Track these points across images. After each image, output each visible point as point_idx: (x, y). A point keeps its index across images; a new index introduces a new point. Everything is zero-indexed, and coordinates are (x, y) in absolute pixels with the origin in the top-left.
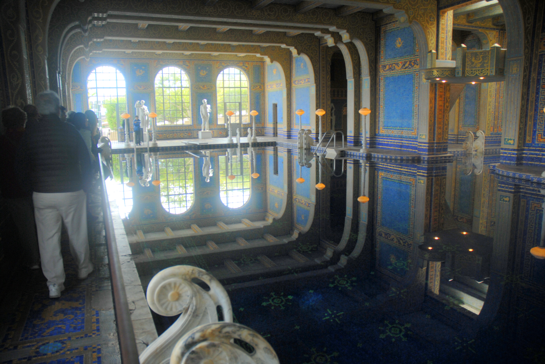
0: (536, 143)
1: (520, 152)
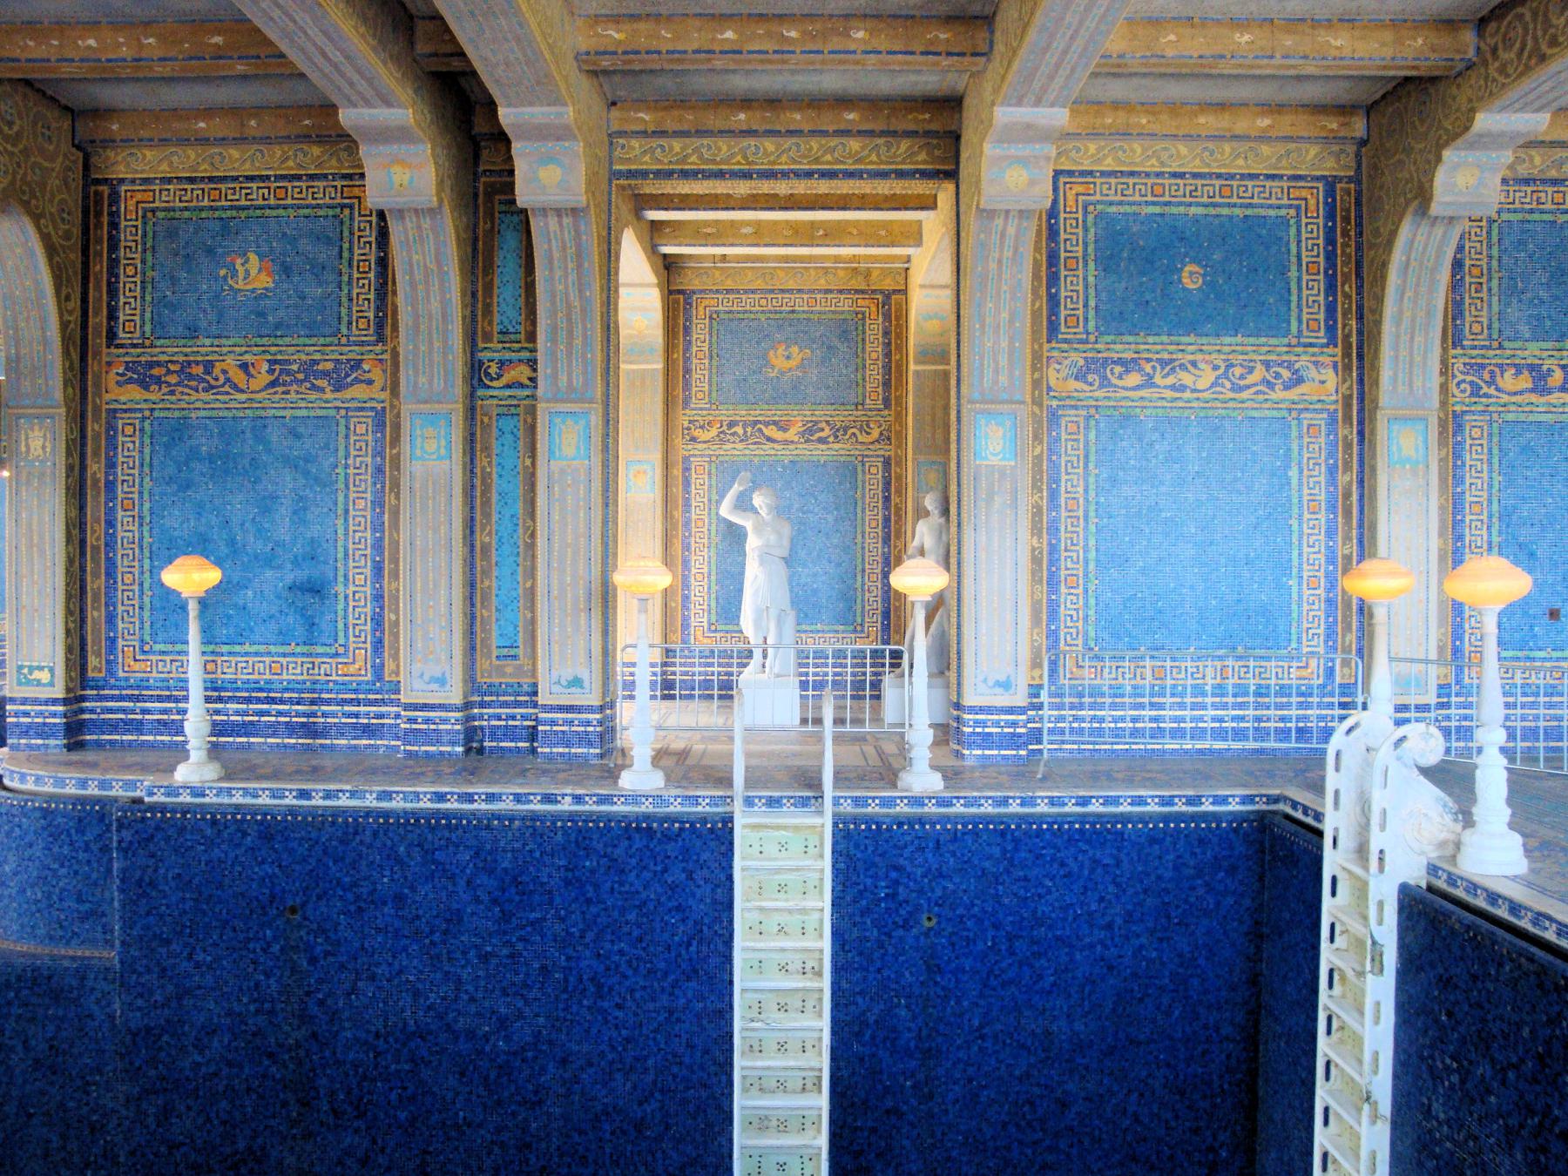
1: (75, 707)
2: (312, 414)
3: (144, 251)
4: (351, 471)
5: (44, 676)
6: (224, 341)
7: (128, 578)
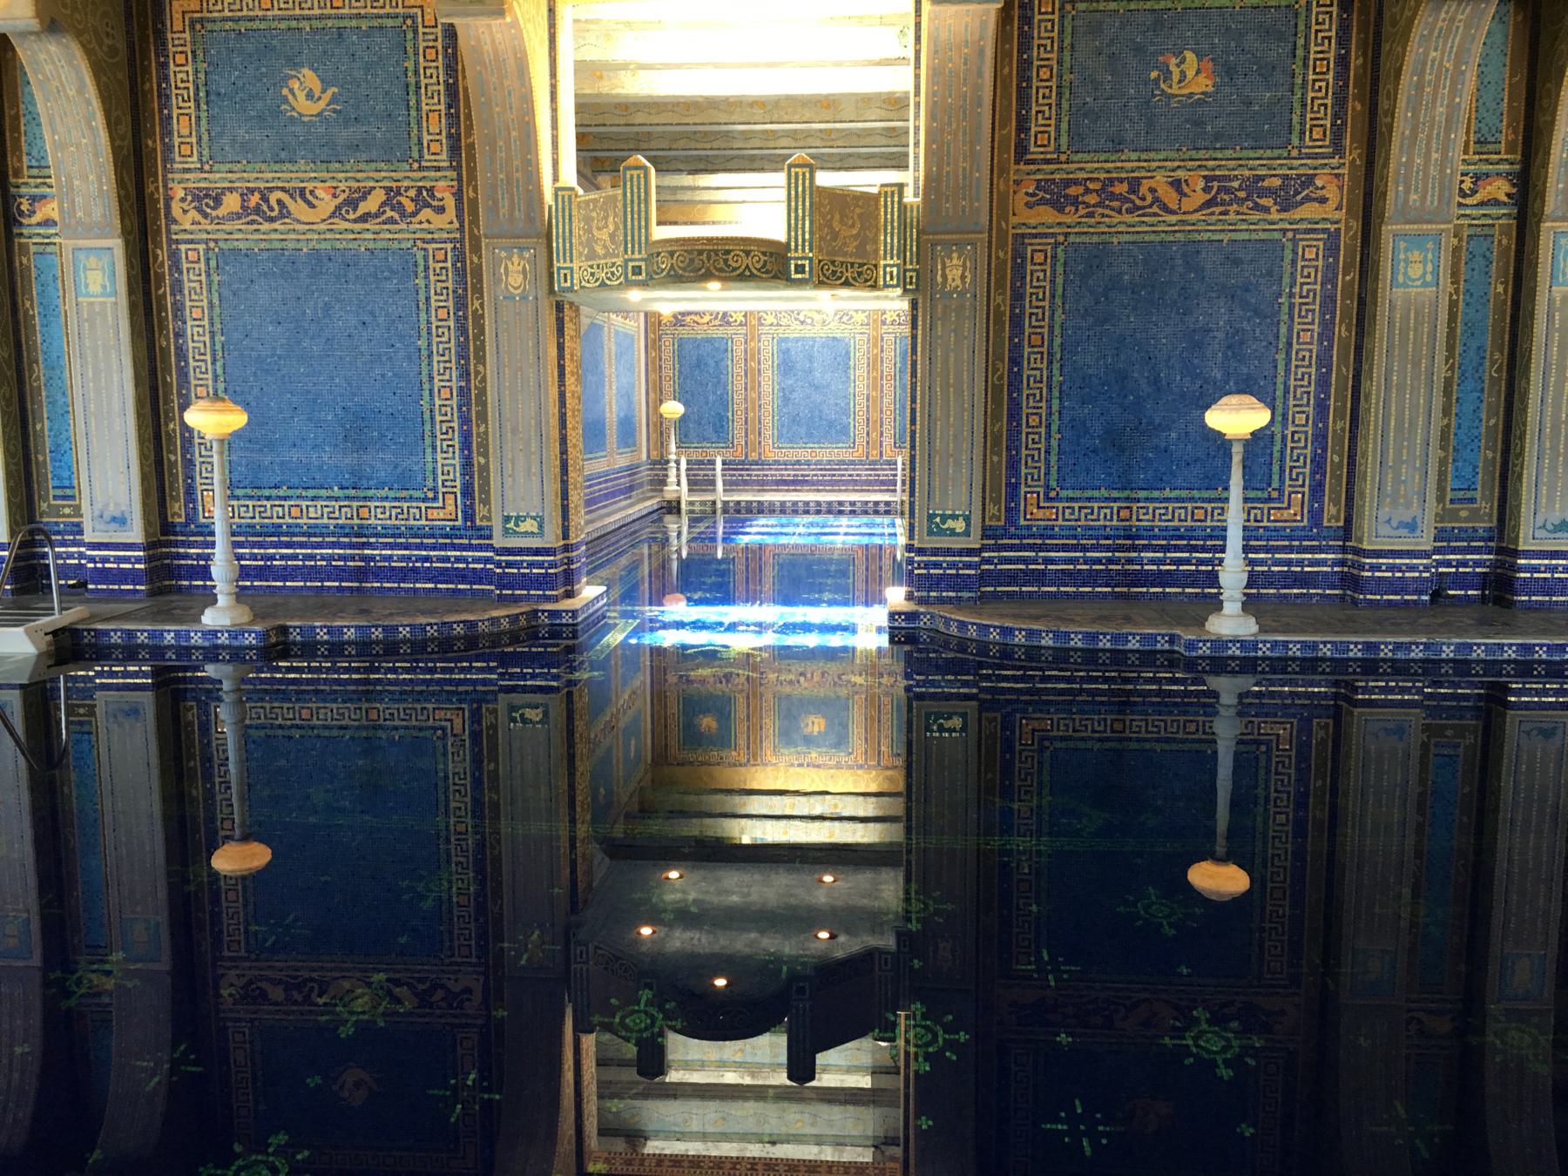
0: (1022, 522)
2: (1254, 236)
3: (1061, 49)
4: (1298, 300)
5: (960, 526)
6: (1152, 155)
7: (1034, 421)
